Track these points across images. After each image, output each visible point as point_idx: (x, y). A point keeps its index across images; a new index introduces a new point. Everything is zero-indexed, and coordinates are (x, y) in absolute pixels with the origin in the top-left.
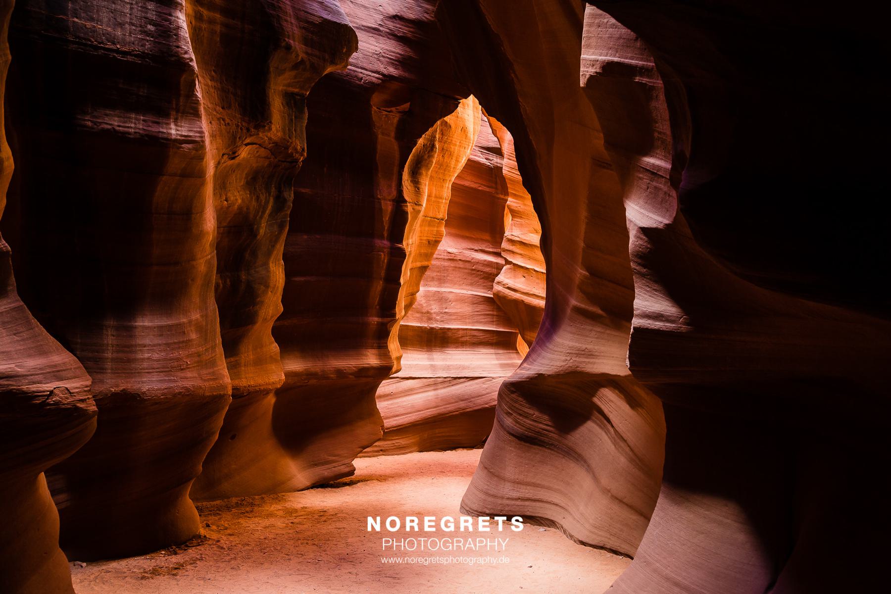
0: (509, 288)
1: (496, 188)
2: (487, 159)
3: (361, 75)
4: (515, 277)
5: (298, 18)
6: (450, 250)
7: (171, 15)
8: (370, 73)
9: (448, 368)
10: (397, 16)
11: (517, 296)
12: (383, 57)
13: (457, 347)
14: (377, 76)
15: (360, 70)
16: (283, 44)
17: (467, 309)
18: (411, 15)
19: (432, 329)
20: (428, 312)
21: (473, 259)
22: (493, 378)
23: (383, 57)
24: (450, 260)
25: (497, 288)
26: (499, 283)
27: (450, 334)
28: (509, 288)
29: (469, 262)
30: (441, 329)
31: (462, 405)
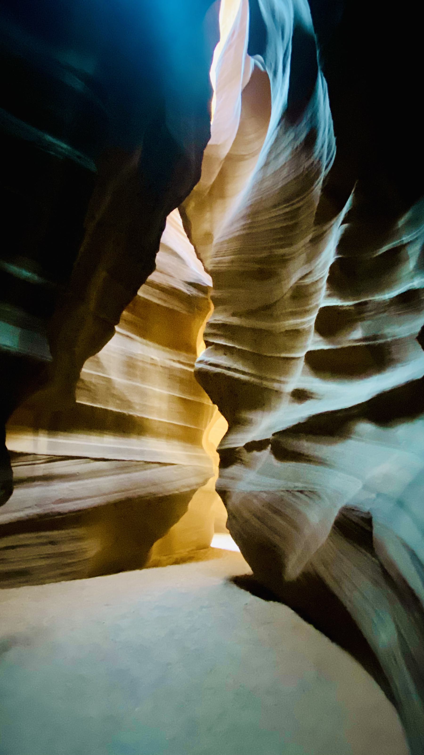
0: (211, 364)
2: (188, 290)
4: (216, 355)
6: (153, 357)
9: (142, 453)
11: (218, 370)
13: (152, 437)
17: (164, 406)
19: (131, 416)
20: (129, 401)
21: (172, 366)
22: (184, 466)
24: (152, 364)
26: (201, 362)
28: (211, 364)
30: (138, 417)
31: (153, 490)
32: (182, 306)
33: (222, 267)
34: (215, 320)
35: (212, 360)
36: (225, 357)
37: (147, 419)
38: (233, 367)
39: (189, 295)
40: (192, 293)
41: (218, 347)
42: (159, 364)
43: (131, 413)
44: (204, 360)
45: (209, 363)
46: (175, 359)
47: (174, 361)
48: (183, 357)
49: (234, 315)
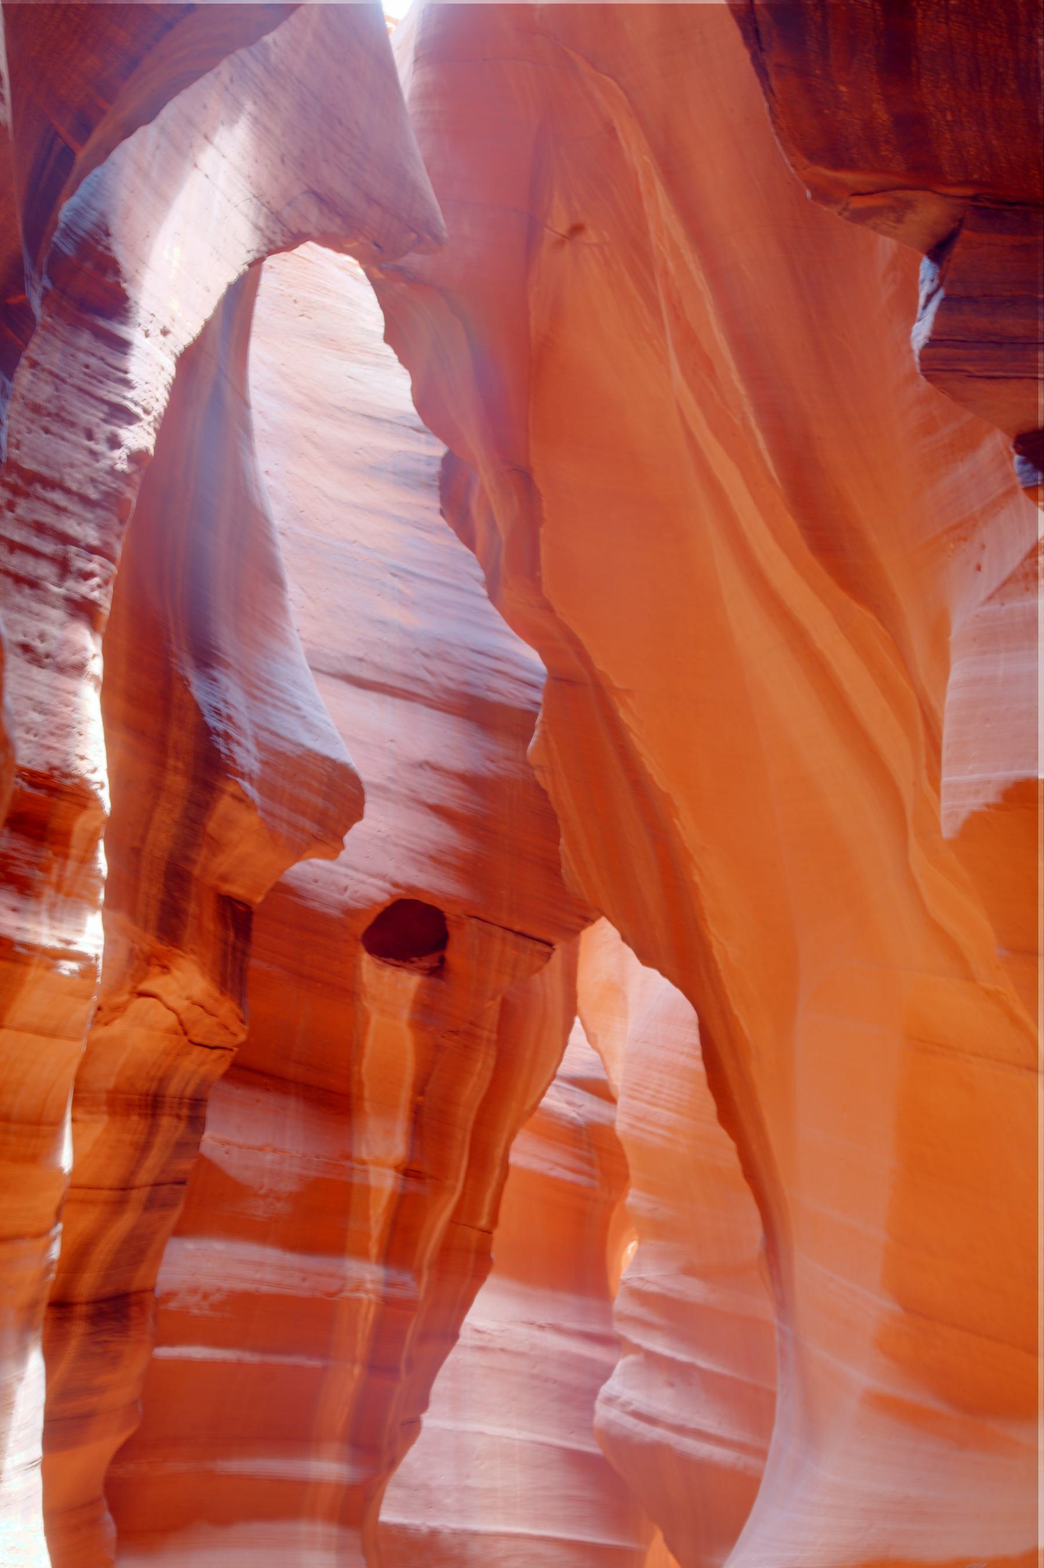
0: (637, 1415)
1: (591, 1176)
2: (569, 1103)
3: (345, 882)
5: (259, 744)
7: (75, 694)
8: (365, 878)
10: (427, 763)
11: (656, 1434)
12: (396, 845)
14: (380, 883)
15: (343, 870)
16: (231, 788)
18: (457, 764)
19: (434, 1533)
23: (396, 845)
25: (604, 1413)
26: (610, 1401)
27: (475, 1548)
28: (637, 1415)
29: (521, 1355)
30: (455, 1533)
32: (554, 1155)
33: (652, 1133)
34: (641, 1279)
35: (638, 1397)
36: (669, 1392)
37: (475, 1534)
38: (692, 1425)
39: (571, 1122)
40: (581, 1111)
41: (652, 1359)
42: (498, 1344)
43: (434, 1523)
44: (618, 1397)
45: (632, 1408)
46: (542, 1321)
47: (541, 1327)
48: (565, 1310)
49: (688, 1271)
